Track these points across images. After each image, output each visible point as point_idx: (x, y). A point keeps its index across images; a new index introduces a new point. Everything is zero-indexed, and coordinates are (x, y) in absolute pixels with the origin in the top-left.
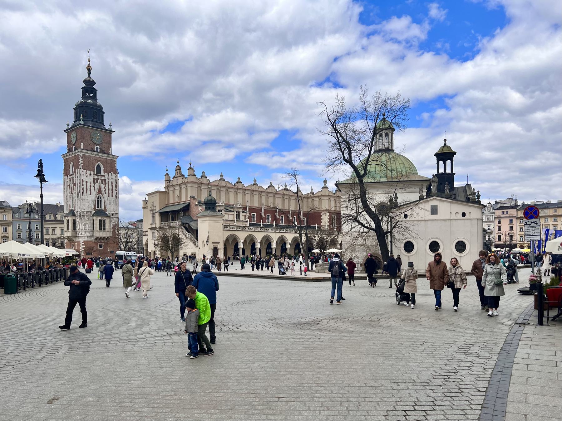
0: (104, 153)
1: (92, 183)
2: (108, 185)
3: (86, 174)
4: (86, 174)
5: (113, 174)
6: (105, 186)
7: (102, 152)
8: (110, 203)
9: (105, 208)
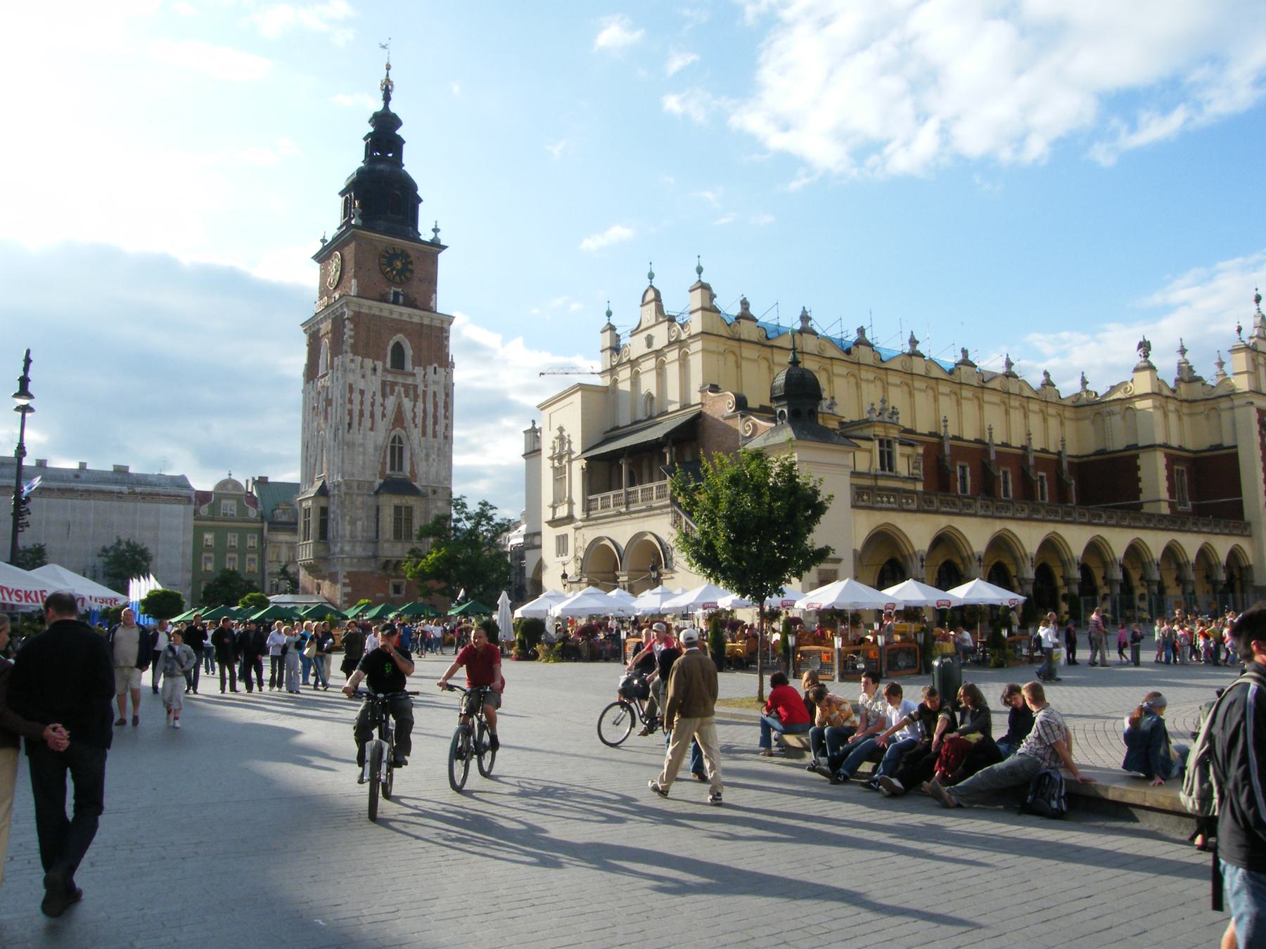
0: (416, 307)
1: (379, 395)
2: (424, 403)
4: (362, 367)
5: (438, 369)
6: (415, 406)
7: (410, 303)
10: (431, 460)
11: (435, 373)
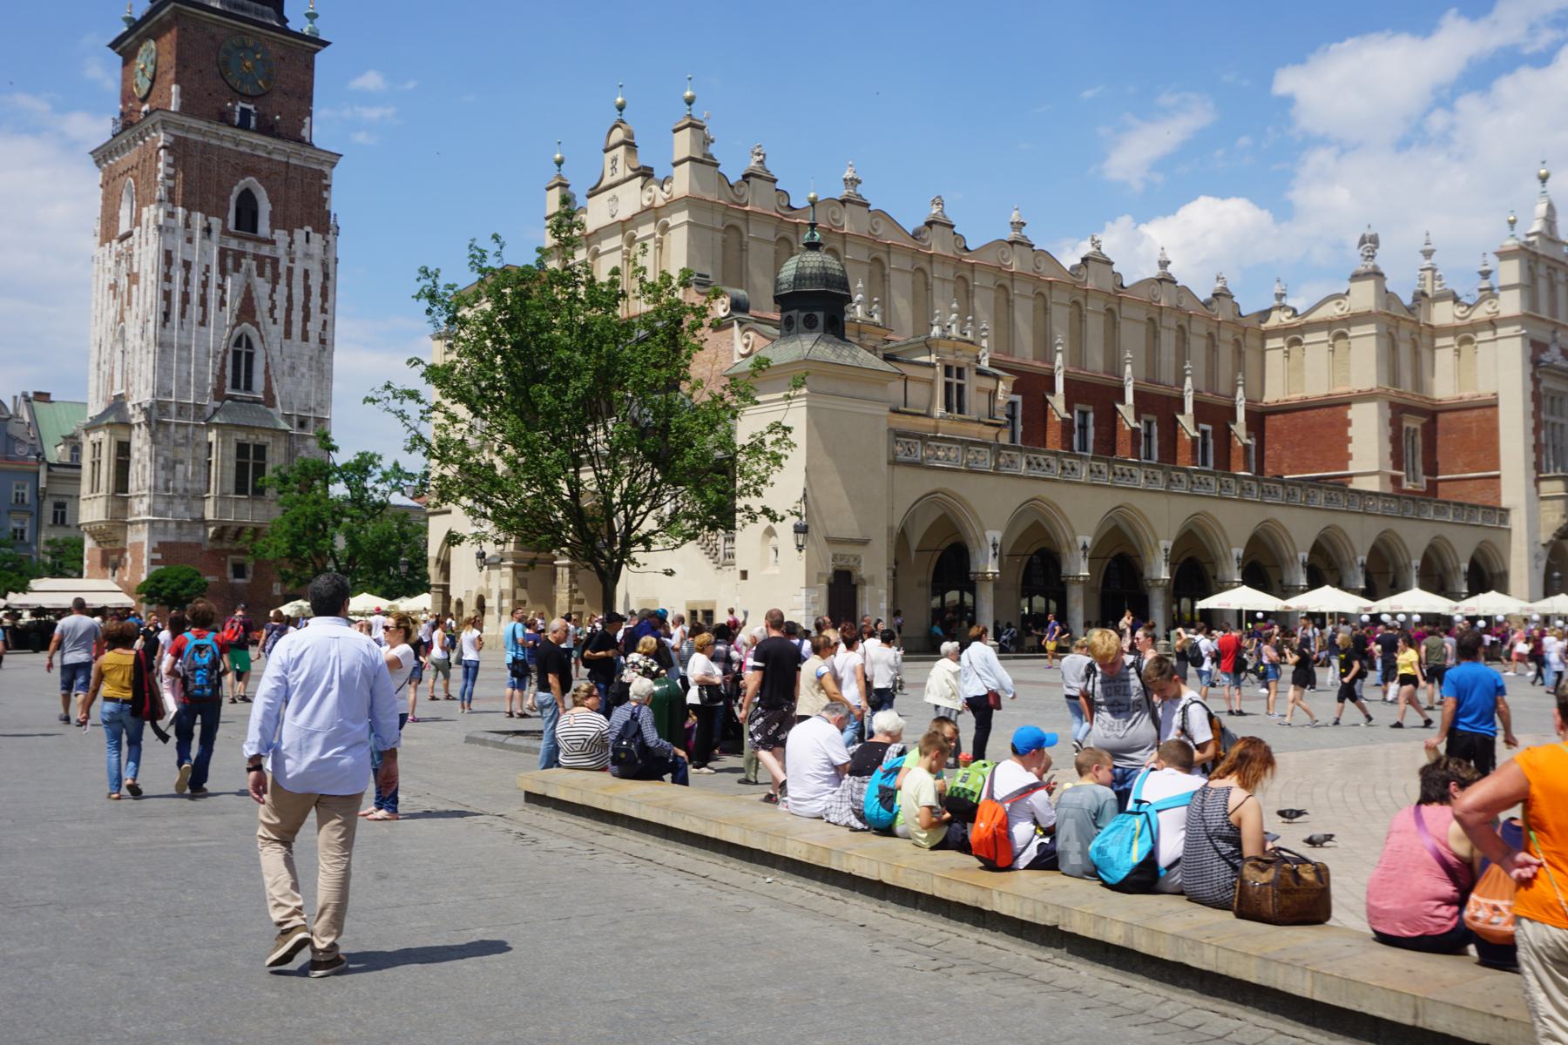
1: (215, 269)
2: (289, 285)
3: (187, 225)
4: (187, 225)
6: (273, 290)
7: (266, 129)
8: (293, 368)
9: (268, 391)
10: (299, 375)
11: (308, 240)
